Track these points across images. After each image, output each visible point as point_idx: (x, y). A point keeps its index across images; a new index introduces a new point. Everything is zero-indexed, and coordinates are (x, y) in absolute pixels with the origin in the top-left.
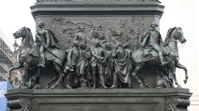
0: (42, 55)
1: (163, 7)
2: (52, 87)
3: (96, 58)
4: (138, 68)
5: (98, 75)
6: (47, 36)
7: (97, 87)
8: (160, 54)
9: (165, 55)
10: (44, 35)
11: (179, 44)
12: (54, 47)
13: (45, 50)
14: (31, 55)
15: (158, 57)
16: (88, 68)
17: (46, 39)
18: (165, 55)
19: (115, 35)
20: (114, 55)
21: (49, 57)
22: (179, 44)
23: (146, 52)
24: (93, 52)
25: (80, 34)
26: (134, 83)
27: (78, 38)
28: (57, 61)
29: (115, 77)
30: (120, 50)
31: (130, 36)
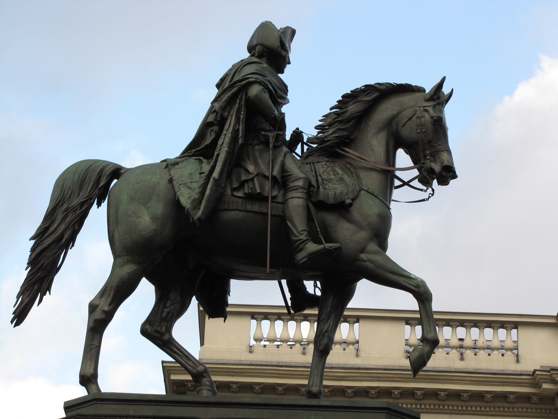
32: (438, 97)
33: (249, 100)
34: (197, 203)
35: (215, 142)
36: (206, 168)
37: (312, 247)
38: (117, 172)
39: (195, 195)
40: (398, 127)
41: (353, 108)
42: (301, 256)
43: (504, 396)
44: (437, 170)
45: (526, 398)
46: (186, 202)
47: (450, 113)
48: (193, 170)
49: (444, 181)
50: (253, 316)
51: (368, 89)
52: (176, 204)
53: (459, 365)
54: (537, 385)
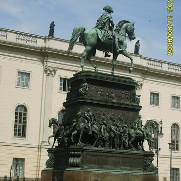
0: (91, 128)
1: (141, 107)
2: (93, 146)
3: (114, 132)
4: (133, 139)
5: (114, 142)
6: (92, 117)
7: (113, 148)
10: (90, 116)
12: (94, 124)
13: (91, 125)
14: (85, 127)
15: (144, 135)
16: (110, 137)
17: (91, 119)
18: (147, 134)
23: (138, 131)
26: (130, 147)
28: (96, 132)
29: (122, 144)
31: (127, 121)
34: (102, 38)
37: (120, 50)
39: (101, 37)
41: (121, 24)
42: (118, 51)
46: (100, 38)
47: (135, 27)
48: (99, 31)
49: (133, 39)
52: (98, 38)
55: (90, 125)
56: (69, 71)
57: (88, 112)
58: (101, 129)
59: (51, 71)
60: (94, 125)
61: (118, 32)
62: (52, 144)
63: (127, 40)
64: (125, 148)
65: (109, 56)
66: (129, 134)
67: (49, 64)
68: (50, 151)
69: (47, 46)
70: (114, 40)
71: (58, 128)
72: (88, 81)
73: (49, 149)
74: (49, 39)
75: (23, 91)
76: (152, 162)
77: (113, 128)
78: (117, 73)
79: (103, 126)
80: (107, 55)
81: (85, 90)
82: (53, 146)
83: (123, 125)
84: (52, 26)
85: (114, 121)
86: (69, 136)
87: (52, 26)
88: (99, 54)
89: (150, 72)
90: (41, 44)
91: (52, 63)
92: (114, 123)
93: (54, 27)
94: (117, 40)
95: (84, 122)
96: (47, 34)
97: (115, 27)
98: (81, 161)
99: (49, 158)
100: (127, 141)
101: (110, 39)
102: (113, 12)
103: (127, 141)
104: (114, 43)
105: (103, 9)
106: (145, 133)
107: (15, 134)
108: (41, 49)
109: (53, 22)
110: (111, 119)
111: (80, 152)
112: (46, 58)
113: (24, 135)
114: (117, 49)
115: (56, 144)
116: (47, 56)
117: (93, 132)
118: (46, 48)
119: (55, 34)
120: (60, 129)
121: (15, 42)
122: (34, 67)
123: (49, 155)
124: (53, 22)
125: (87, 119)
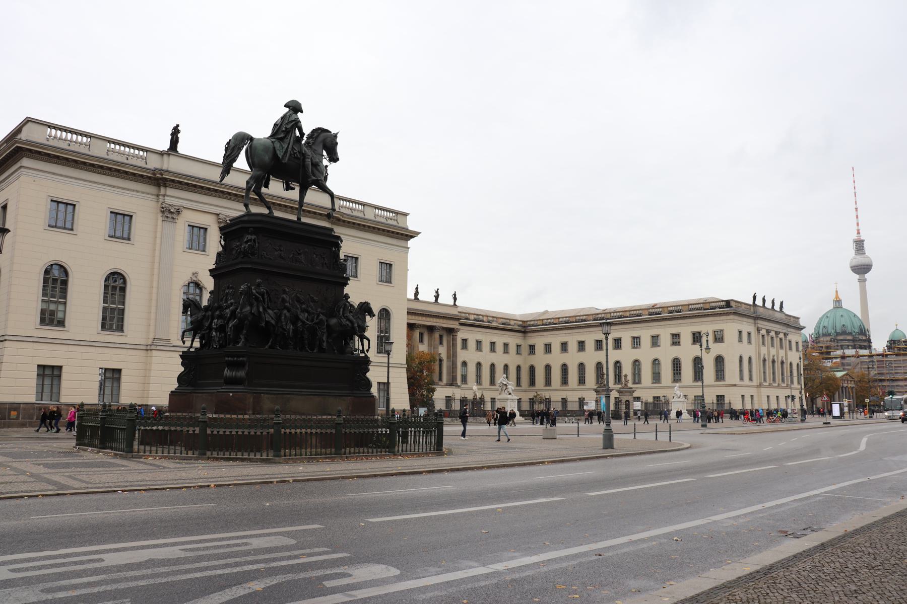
3: (303, 322)
8: (356, 325)
9: (359, 326)
11: (368, 318)
12: (269, 308)
13: (264, 309)
14: (253, 314)
15: (353, 328)
16: (296, 331)
18: (359, 326)
19: (314, 301)
20: (315, 321)
21: (268, 318)
22: (368, 318)
23: (344, 321)
24: (301, 317)
25: (284, 296)
27: (284, 300)
28: (273, 322)
30: (321, 317)
32: (335, 136)
33: (288, 126)
35: (284, 137)
36: (285, 146)
38: (252, 139)
40: (326, 142)
41: (316, 135)
43: (142, 176)
44: (334, 158)
45: (150, 178)
46: (280, 154)
48: (277, 145)
50: (49, 127)
51: (319, 129)
53: (126, 161)
54: (154, 174)
55: (261, 310)
56: (235, 210)
57: (259, 285)
58: (280, 316)
59: (172, 213)
60: (270, 311)
61: (310, 147)
62: (188, 344)
63: (325, 162)
64: (322, 350)
65: (293, 189)
66: (328, 326)
67: (168, 200)
68: (186, 357)
69: (165, 168)
70: (304, 160)
71: (200, 315)
72: (256, 231)
73: (183, 352)
74: (169, 155)
75: (118, 246)
76: (368, 374)
77: (303, 316)
78: (304, 220)
79: (285, 311)
80: (288, 188)
81: (253, 247)
82: (191, 347)
83: (319, 310)
84: (176, 131)
85: (303, 303)
86: (222, 329)
87: (176, 131)
88: (275, 188)
89: (344, 221)
90: (154, 163)
91: (174, 197)
92: (304, 306)
93: (179, 135)
94: (308, 162)
95: (251, 305)
96: (165, 146)
97: (305, 138)
98: (247, 374)
99: (182, 369)
100: (324, 338)
101: (297, 158)
102: (302, 112)
103: (324, 338)
104: (304, 166)
105: (286, 106)
106: (356, 325)
107: (103, 327)
108: (154, 171)
109: (178, 126)
110: (299, 300)
111: (245, 359)
112: (163, 191)
113: (120, 328)
114: (309, 177)
115: (197, 344)
116: (165, 186)
117: (267, 323)
118: (162, 171)
119: (181, 148)
120: (204, 316)
121: (107, 157)
122: (140, 203)
123: (183, 364)
124: (178, 126)
125: (257, 299)
